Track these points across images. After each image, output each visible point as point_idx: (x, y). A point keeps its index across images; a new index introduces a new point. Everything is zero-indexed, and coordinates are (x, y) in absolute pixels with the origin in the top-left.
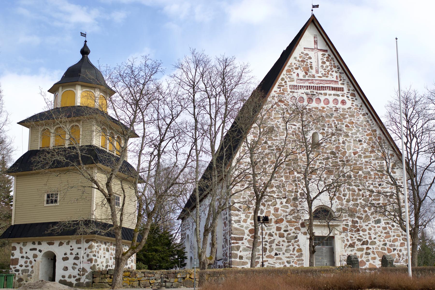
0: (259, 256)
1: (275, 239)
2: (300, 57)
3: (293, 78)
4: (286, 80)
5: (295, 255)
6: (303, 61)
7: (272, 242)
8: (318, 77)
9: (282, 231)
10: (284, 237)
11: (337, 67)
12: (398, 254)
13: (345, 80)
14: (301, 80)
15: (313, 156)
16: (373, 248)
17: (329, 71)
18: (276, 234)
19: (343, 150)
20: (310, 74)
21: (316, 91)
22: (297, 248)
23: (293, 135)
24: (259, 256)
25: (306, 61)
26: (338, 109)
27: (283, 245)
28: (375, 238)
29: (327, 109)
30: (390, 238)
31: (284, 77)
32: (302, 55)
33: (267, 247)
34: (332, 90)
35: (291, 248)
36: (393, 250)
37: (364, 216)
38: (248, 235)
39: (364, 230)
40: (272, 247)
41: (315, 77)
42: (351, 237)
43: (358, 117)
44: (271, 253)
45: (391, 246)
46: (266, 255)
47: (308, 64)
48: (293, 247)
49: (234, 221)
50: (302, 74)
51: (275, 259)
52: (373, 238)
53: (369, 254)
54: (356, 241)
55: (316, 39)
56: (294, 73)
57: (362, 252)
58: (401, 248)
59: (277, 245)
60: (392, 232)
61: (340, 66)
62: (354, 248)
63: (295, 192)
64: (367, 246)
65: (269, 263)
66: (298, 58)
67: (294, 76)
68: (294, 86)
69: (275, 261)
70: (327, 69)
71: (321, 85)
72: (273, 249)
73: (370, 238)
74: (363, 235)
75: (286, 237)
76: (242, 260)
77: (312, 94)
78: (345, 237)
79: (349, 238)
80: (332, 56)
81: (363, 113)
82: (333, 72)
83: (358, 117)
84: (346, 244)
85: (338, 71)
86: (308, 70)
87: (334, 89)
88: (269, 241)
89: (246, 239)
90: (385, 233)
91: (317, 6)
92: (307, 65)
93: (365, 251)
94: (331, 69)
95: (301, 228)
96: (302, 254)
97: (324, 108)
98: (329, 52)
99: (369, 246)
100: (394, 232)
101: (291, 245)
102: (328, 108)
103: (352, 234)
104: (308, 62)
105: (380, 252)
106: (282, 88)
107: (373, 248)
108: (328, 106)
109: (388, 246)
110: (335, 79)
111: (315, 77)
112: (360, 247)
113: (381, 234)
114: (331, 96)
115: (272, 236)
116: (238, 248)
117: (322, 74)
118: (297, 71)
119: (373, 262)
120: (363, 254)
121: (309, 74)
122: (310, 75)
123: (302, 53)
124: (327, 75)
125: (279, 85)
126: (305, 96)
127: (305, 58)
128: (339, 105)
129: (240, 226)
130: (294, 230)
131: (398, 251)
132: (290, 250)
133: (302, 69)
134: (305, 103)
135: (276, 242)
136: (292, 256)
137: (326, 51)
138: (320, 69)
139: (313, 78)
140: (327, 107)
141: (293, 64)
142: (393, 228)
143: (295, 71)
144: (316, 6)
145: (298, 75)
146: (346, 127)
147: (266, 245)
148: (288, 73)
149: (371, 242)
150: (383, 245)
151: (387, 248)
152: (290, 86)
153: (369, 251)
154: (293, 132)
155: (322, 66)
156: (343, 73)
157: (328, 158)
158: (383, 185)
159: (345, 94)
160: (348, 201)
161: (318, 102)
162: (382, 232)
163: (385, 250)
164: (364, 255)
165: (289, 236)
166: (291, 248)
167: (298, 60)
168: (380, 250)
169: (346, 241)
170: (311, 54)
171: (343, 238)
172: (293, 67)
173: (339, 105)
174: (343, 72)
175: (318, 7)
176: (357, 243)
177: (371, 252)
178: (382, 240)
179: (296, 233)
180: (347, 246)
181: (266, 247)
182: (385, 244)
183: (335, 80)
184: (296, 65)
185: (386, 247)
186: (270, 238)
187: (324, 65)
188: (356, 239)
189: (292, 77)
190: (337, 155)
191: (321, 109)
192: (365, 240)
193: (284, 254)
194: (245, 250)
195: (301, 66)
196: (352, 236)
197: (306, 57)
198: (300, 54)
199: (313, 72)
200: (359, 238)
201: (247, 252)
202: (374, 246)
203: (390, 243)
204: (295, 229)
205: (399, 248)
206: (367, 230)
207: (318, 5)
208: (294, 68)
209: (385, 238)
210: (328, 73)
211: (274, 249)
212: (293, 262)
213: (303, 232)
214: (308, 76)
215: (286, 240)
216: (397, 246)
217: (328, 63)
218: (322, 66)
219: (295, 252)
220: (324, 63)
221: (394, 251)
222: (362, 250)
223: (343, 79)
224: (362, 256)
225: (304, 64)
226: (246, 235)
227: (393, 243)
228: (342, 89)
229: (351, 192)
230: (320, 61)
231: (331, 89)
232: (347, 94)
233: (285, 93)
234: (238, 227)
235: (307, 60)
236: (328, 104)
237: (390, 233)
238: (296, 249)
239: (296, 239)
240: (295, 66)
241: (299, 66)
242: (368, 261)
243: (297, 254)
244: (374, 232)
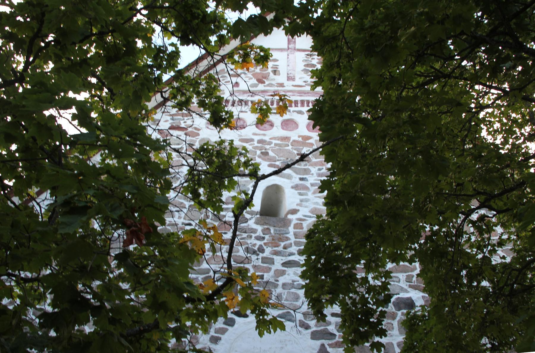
8: (293, 86)
15: (259, 243)
20: (273, 82)
41: (284, 86)
111: (284, 86)
121: (267, 83)
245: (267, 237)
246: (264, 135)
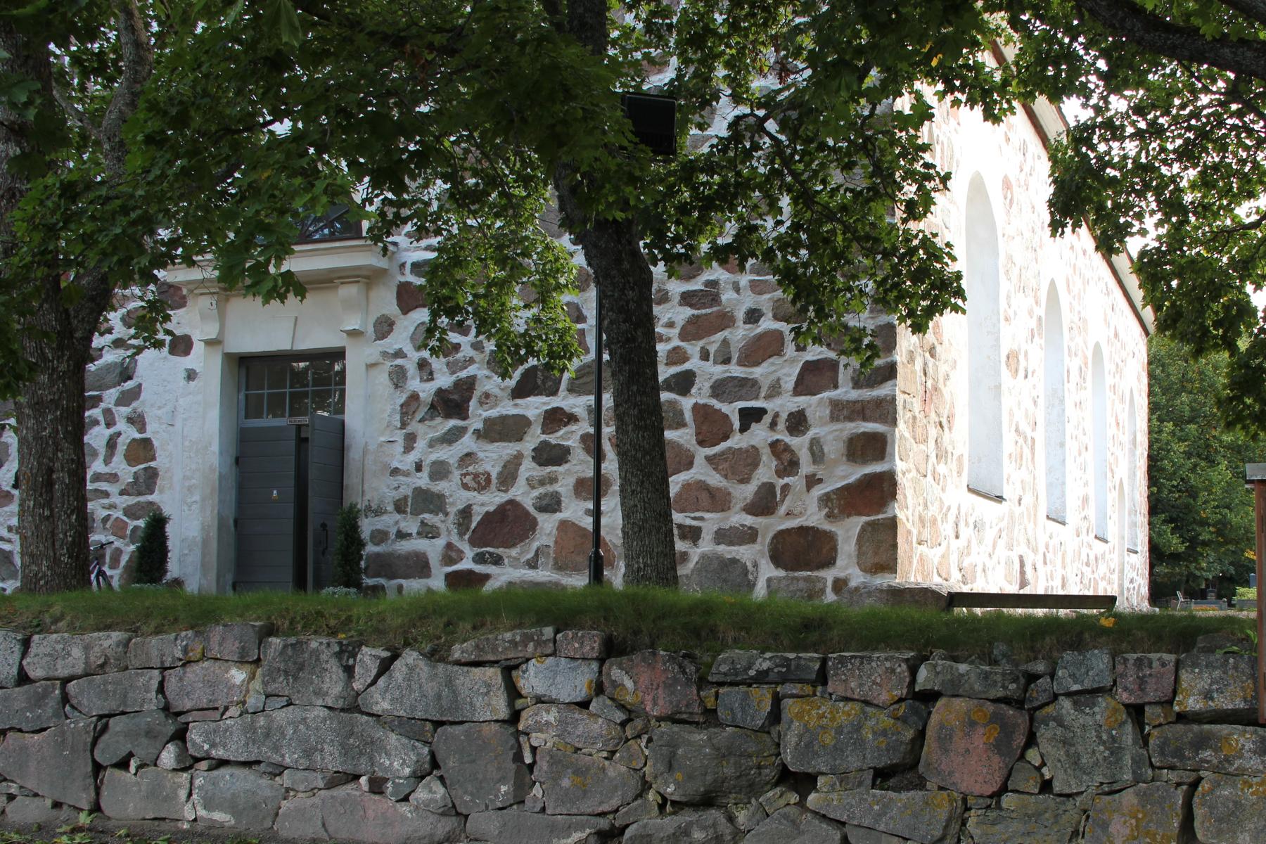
5: (113, 478)
12: (777, 448)
30: (719, 336)
36: (737, 425)
45: (721, 389)
58: (802, 401)
62: (464, 416)
64: (555, 402)
78: (408, 348)
90: (687, 299)
93: (535, 437)
96: (152, 475)
112: (508, 408)
119: (908, 520)
120: (518, 458)
131: (781, 425)
164: (528, 468)
171: (399, 354)
177: (573, 442)
203: (718, 371)
205: (787, 403)
209: (684, 336)
221: (744, 429)
224: (508, 476)
237: (727, 296)
238: (121, 447)
239: (129, 385)
242: (551, 504)
243: (127, 472)
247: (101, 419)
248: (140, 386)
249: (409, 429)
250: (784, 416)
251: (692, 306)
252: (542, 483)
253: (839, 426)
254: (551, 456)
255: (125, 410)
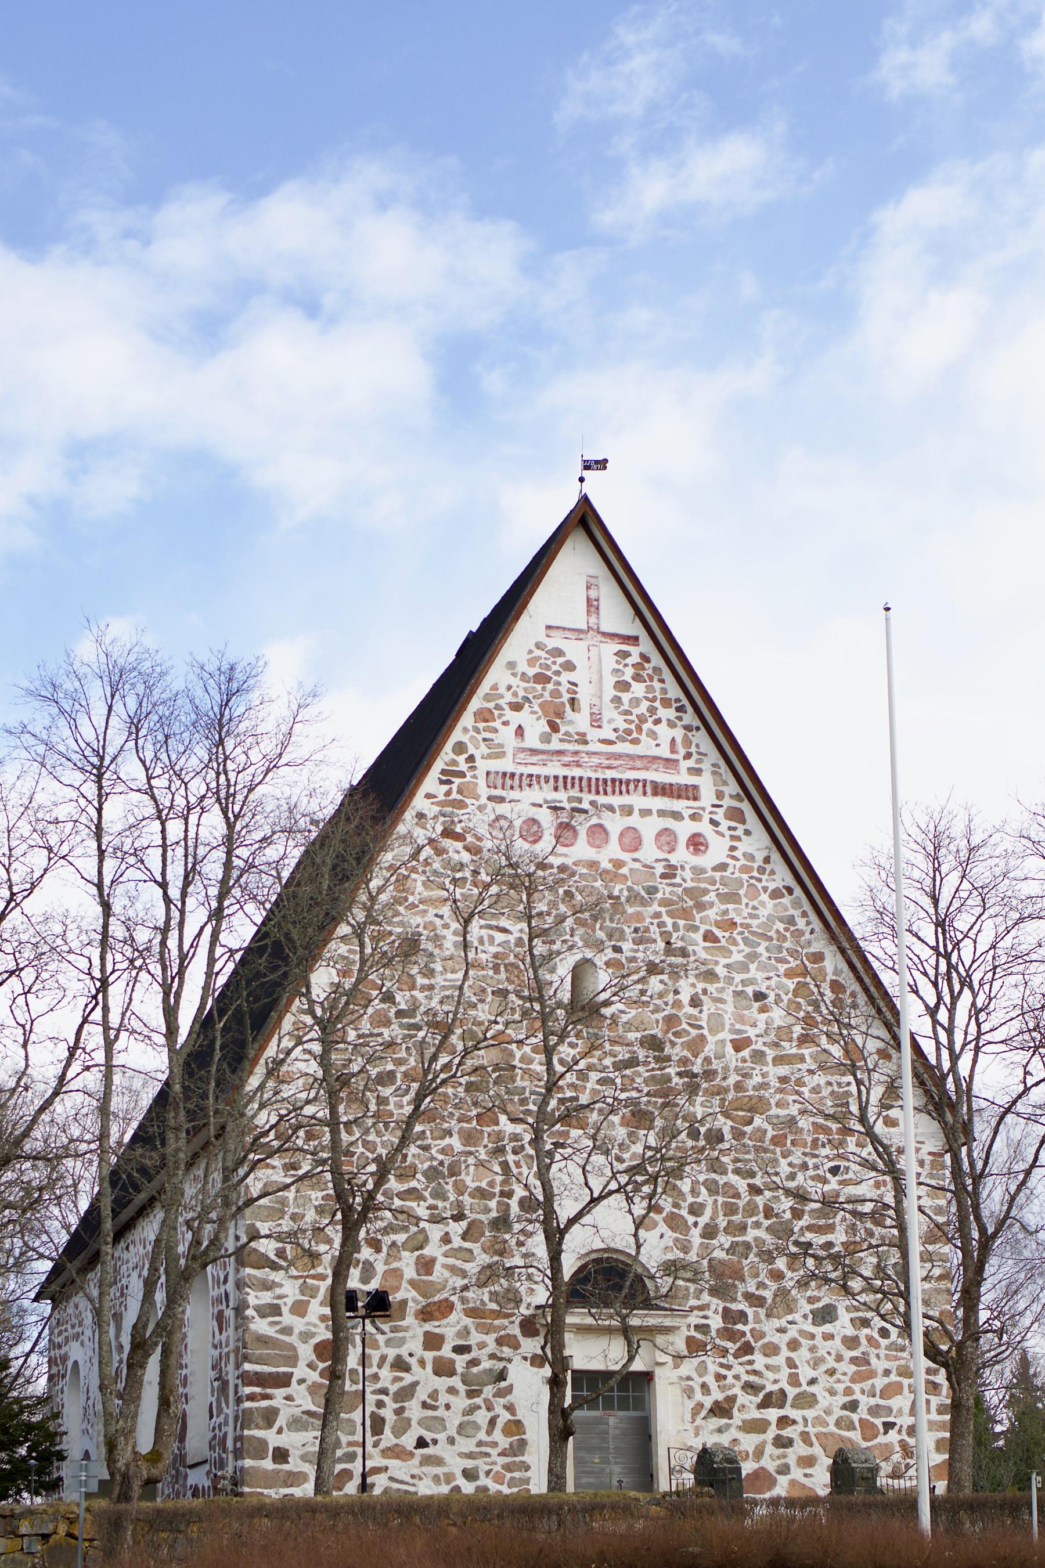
0: (351, 1449)
1: (417, 1383)
2: (532, 662)
3: (501, 746)
4: (471, 750)
5: (495, 1444)
6: (541, 679)
7: (406, 1393)
8: (599, 741)
9: (446, 1351)
10: (452, 1373)
11: (675, 705)
12: (903, 1444)
13: (705, 755)
14: (534, 752)
15: (572, 1052)
16: (805, 1420)
17: (642, 719)
18: (422, 1363)
19: (694, 1032)
20: (570, 729)
21: (592, 797)
22: (505, 1416)
23: (496, 968)
24: (351, 1449)
25: (555, 678)
26: (675, 868)
27: (448, 1407)
28: (813, 1382)
29: (631, 870)
30: (871, 1382)
31: (465, 739)
32: (538, 653)
33: (388, 1413)
34: (655, 793)
35: (482, 1417)
36: (882, 1430)
37: (768, 1294)
38: (311, 1366)
39: (772, 1350)
40: (406, 1414)
41: (586, 742)
42: (719, 1377)
43: (755, 903)
44: (403, 1438)
45: (874, 1410)
46: (383, 1445)
47: (563, 689)
48: (490, 1415)
49: (258, 1309)
50: (535, 727)
51: (416, 1461)
52: (803, 1381)
53: (788, 1443)
54: (737, 1390)
55: (593, 594)
56: (505, 723)
57: (762, 1437)
59: (425, 1405)
60: (878, 1356)
61: (685, 701)
62: (731, 1418)
63: (502, 1194)
64: (782, 1412)
65: (391, 1479)
66: (523, 667)
67: (506, 736)
68: (504, 774)
69: (415, 1471)
70: (636, 711)
71: (610, 774)
72: (409, 1420)
73: (794, 1380)
74: (767, 1367)
75: (462, 1375)
76: (285, 1467)
77: (574, 810)
78: (695, 1375)
79: (710, 1380)
80: (657, 660)
81: (772, 886)
82: (657, 722)
83: (755, 903)
84: (700, 1405)
85: (680, 719)
86: (560, 715)
87: (660, 790)
88: (393, 1388)
89: (301, 1381)
90: (854, 1360)
91: (602, 464)
92: (556, 694)
93: (772, 1432)
94: (652, 710)
95: (520, 1338)
96: (523, 1443)
97: (618, 864)
98: (646, 645)
99: (789, 1411)
100: (888, 1358)
101: (479, 1407)
102: (637, 865)
103: (722, 1365)
104: (559, 684)
105: (832, 1434)
106: (457, 781)
107: (805, 1420)
108: (636, 855)
109: (863, 1412)
110: (664, 752)
111: (586, 742)
112: (756, 1414)
113: (836, 1365)
114: (648, 819)
115: (407, 1369)
116: (269, 1417)
117: (615, 730)
118: (515, 718)
120: (764, 1443)
121: (562, 731)
122: (566, 734)
123: (539, 646)
124: (635, 735)
125: (443, 772)
126: (545, 816)
127: (548, 667)
128: (682, 855)
129: (278, 1328)
130: (492, 1347)
131: (904, 1432)
132: (478, 1427)
133: (536, 708)
134: (547, 841)
135: (421, 1394)
136: (483, 1449)
137: (634, 640)
138: (609, 713)
139: (581, 748)
140: (634, 860)
141: (502, 690)
142: (884, 1342)
143: (509, 715)
144: (597, 462)
145: (520, 731)
146: (705, 938)
147: (380, 1404)
148: (481, 725)
149: (798, 1396)
150: (844, 1407)
151: (861, 1420)
152: (488, 773)
153: (788, 1432)
154: (496, 956)
155: (617, 700)
156: (698, 729)
157: (632, 1062)
158: (847, 1169)
159: (703, 809)
160: (710, 1232)
161: (597, 842)
162: (839, 1358)
163: (851, 1427)
164: (770, 1449)
165: (475, 1370)
166: (482, 1417)
167: (523, 674)
168: (832, 1428)
169: (698, 1390)
170: (574, 650)
171: (689, 1378)
172: (502, 702)
173: (682, 855)
174: (697, 722)
175: (605, 468)
176: (743, 1398)
177: (795, 1436)
178: (840, 1387)
179: (501, 1359)
180: (704, 1413)
181: (382, 1412)
182: (853, 1406)
183: (667, 755)
184: (515, 694)
185: (855, 1417)
186: (397, 1379)
187: (626, 697)
188: (739, 1385)
189: (497, 738)
190: (668, 1050)
191: (610, 866)
192: (775, 1388)
193: (451, 1441)
194: (296, 1424)
195: (534, 697)
196: (723, 1372)
197: (554, 663)
198: (530, 652)
199: (580, 721)
200: (752, 1378)
201: (304, 1433)
202: (810, 1414)
203: (873, 1401)
204: (500, 1342)
206: (784, 1348)
207: (606, 461)
208: (506, 707)
209: (853, 1380)
210: (639, 729)
211: (414, 1423)
212: (488, 1473)
213: (529, 1355)
214: (560, 735)
215: (462, 1388)
216: (900, 1411)
217: (638, 689)
218: (617, 700)
219: (498, 1435)
220: (623, 686)
221: (886, 1433)
222: (757, 1426)
223: (699, 753)
224: (759, 1452)
225: (544, 689)
226: (302, 1364)
227: (882, 1402)
228: (691, 793)
229: (720, 1200)
230: (610, 681)
231: (649, 789)
232: (711, 813)
233: (468, 801)
234: (271, 1332)
235: (558, 673)
236: (636, 850)
237: (874, 1361)
238: (500, 1423)
239: (503, 1384)
240: (509, 697)
241: (526, 699)
242: (784, 1470)
243: (504, 1442)
244: (808, 1355)
245: (580, 1042)
246: (565, 855)
247: (483, 1405)
248: (512, 1385)
249: (697, 1423)
250: (905, 1427)
251: (856, 1365)
252: (779, 1458)
253: (933, 1433)
254: (783, 1443)
255: (502, 1401)
